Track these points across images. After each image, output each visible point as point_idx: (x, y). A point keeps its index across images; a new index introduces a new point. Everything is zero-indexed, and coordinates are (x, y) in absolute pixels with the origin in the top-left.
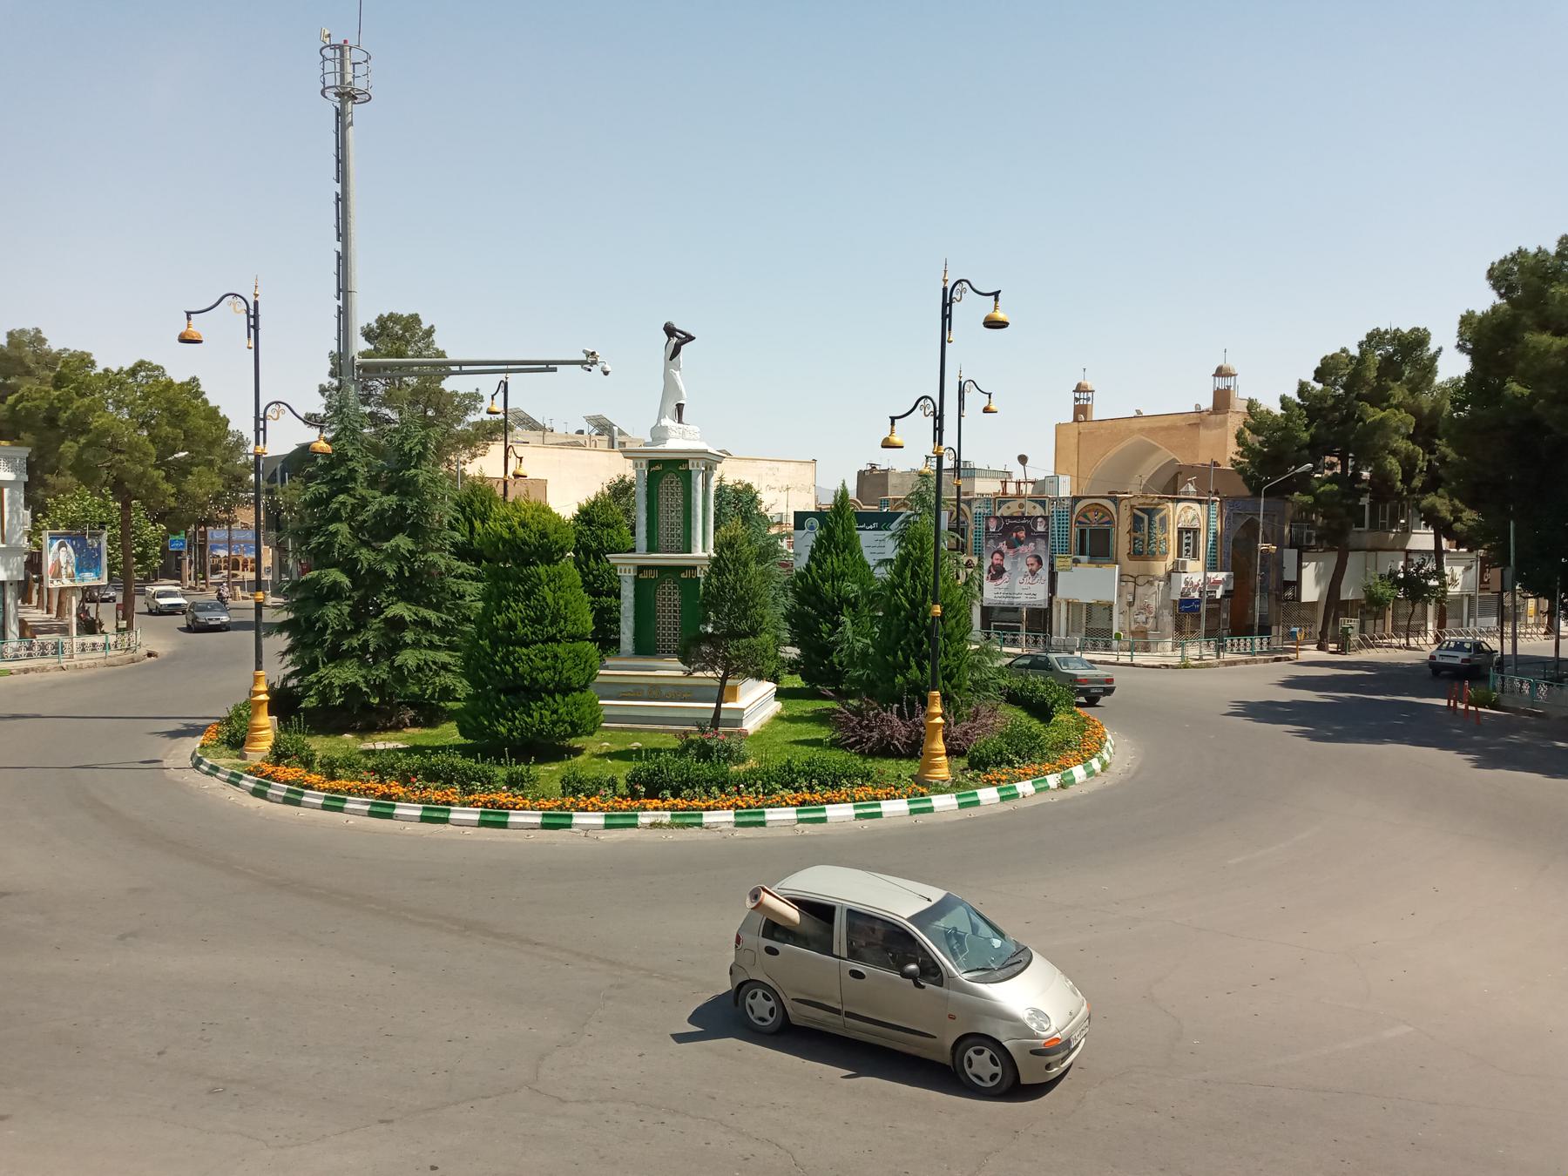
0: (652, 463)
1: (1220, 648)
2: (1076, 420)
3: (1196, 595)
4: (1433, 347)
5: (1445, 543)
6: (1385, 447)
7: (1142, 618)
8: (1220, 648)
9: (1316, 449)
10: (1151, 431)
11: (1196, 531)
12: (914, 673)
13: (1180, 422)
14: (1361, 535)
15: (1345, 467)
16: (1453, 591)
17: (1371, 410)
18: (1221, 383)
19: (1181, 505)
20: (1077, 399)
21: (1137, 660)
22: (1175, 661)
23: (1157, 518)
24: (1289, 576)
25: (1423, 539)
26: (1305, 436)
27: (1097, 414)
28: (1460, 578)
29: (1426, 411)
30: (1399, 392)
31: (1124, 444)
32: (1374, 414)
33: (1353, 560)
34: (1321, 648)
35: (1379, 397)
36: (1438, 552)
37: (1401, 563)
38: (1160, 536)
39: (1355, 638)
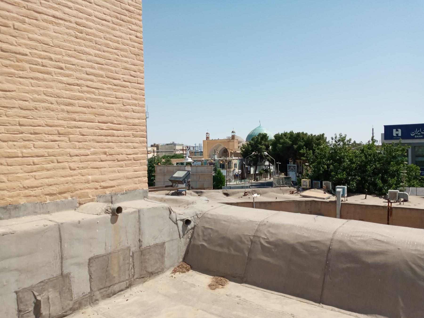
0: (186, 163)
1: (241, 182)
2: (207, 139)
3: (237, 174)
4: (268, 136)
5: (270, 164)
6: (262, 151)
7: (230, 177)
8: (241, 182)
9: (252, 151)
10: (221, 142)
11: (236, 164)
12: (221, 186)
13: (226, 141)
14: (259, 163)
15: (256, 153)
16: (272, 171)
17: (260, 146)
18: (233, 134)
19: (234, 160)
20: (207, 136)
21: (230, 184)
22: (236, 184)
23: (231, 162)
24: (249, 170)
25: (267, 163)
26: (251, 149)
27: (210, 139)
28: (273, 169)
29: (267, 144)
30: (263, 142)
31: (216, 145)
32: (260, 146)
33: (258, 167)
34: (254, 181)
35: (260, 143)
36: (269, 165)
37: (264, 167)
38: (232, 165)
39: (259, 179)
